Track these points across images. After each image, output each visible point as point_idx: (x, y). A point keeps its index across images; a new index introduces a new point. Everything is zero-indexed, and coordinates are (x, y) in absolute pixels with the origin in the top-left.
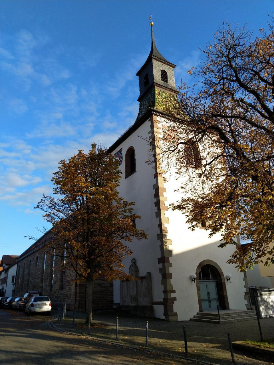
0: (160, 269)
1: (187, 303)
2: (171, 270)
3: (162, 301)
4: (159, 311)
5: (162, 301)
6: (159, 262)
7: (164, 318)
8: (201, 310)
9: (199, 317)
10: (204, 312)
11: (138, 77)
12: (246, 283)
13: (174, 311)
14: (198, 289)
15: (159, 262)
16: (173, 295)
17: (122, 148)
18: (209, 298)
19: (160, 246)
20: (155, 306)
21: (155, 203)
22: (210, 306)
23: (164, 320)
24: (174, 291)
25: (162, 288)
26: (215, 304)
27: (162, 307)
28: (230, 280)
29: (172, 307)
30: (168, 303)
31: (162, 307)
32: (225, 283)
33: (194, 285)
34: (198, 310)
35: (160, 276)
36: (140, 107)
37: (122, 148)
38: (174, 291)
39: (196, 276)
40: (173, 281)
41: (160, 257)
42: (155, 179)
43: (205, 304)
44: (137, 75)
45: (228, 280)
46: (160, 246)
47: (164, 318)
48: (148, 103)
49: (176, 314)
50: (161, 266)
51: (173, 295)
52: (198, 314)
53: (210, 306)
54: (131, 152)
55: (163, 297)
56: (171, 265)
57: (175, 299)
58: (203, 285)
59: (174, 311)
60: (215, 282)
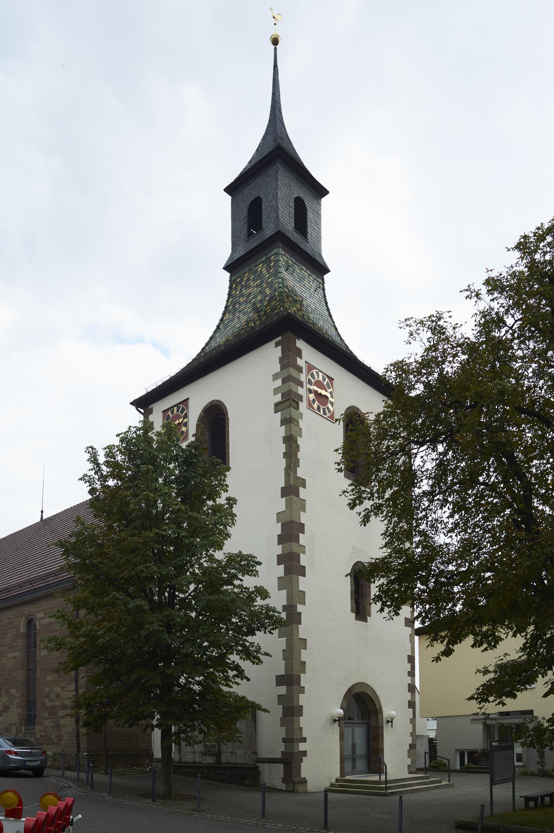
0: (279, 696)
1: (322, 762)
2: (303, 700)
3: (279, 756)
4: (273, 775)
5: (279, 756)
6: (278, 684)
7: (283, 786)
8: (342, 774)
9: (340, 786)
10: (347, 778)
11: (228, 198)
12: (414, 728)
13: (302, 776)
14: (342, 738)
15: (278, 684)
16: (302, 747)
17: (188, 399)
18: (354, 752)
19: (283, 650)
20: (260, 765)
21: (278, 556)
22: (354, 767)
23: (281, 790)
24: (304, 740)
25: (282, 732)
26: (361, 764)
27: (281, 767)
28: (392, 722)
29: (300, 766)
30: (291, 760)
31: (281, 767)
32: (382, 727)
33: (336, 729)
34: (337, 774)
35: (277, 711)
36: (231, 288)
37: (188, 399)
38: (304, 740)
39: (342, 711)
40: (303, 721)
41: (283, 672)
42: (284, 498)
43: (348, 766)
44: (229, 190)
45: (388, 722)
46: (283, 650)
47: (283, 786)
48: (257, 286)
49: (304, 781)
50: (283, 690)
51: (302, 747)
52: (337, 780)
53: (354, 767)
54: (216, 418)
55: (283, 750)
56: (302, 690)
57: (304, 753)
58: (348, 731)
59: (302, 776)
60: (366, 725)
